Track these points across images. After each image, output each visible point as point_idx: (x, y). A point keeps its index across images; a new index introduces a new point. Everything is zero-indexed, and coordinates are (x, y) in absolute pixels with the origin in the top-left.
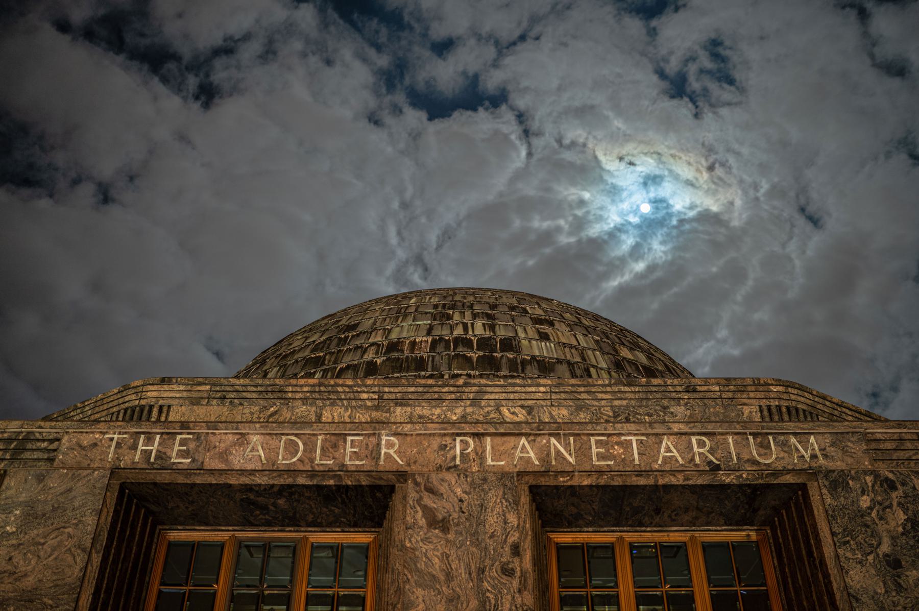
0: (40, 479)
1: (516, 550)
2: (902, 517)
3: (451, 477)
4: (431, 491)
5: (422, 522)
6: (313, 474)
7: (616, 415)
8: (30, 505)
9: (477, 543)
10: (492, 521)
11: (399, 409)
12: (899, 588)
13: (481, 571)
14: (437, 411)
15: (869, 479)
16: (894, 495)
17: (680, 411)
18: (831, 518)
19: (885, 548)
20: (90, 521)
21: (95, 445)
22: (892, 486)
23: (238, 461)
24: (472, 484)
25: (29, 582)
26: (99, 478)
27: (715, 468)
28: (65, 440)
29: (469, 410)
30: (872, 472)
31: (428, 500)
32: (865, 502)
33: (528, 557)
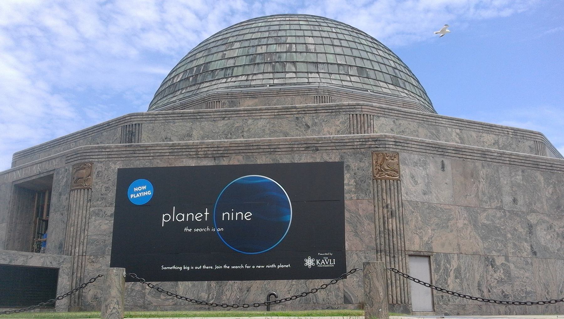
2: (65, 180)
17: (105, 134)
19: (60, 191)
30: (64, 167)
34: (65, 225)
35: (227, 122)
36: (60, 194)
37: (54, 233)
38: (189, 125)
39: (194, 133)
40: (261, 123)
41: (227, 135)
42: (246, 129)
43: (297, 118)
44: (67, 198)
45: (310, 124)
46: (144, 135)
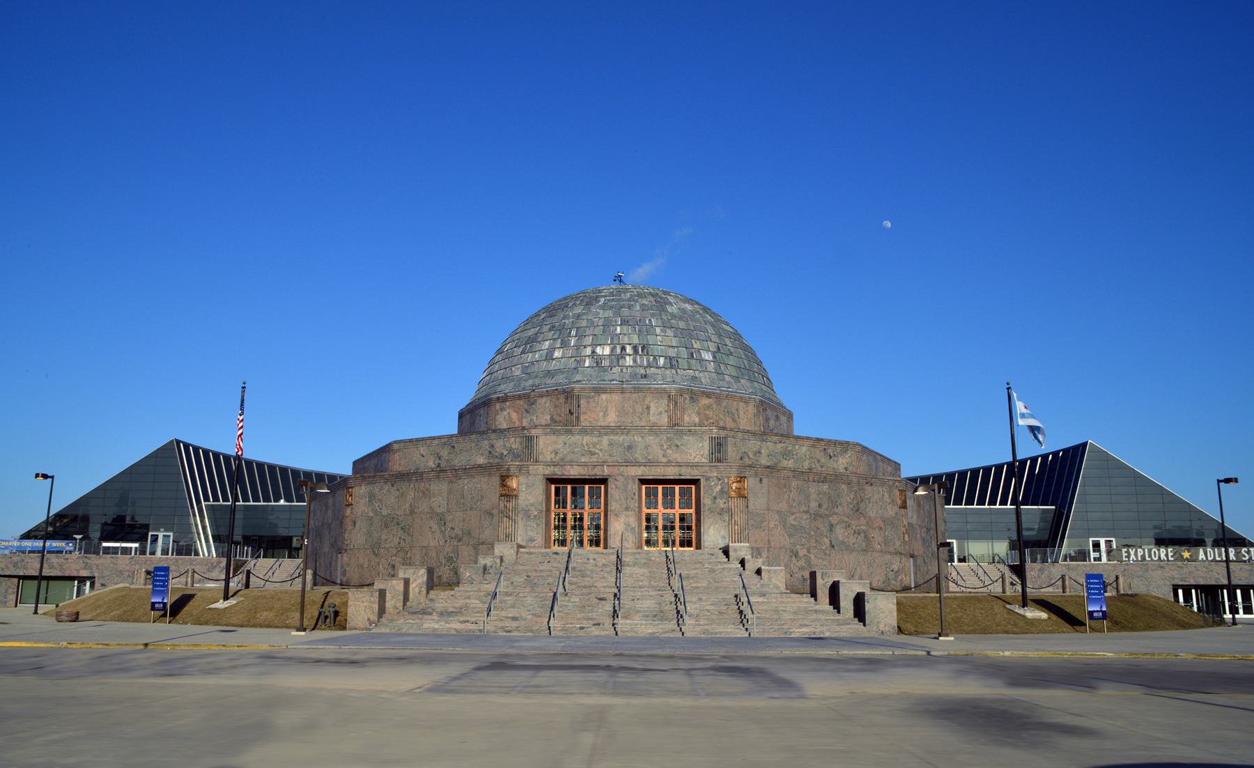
0: (527, 477)
1: (634, 494)
2: (720, 487)
3: (620, 477)
4: (616, 480)
5: (614, 487)
6: (590, 475)
7: (667, 439)
8: (526, 484)
9: (626, 492)
10: (630, 487)
11: (605, 437)
12: (715, 503)
13: (627, 498)
14: (616, 437)
15: (715, 478)
16: (720, 482)
18: (704, 487)
19: (714, 494)
20: (541, 487)
21: (538, 468)
22: (720, 480)
23: (572, 473)
24: (625, 479)
25: (531, 501)
26: (541, 477)
27: (680, 475)
28: (531, 467)
29: (626, 437)
30: (717, 477)
31: (616, 482)
32: (713, 484)
33: (637, 496)
34: (727, 524)
35: (783, 445)
36: (715, 498)
37: (712, 527)
38: (759, 443)
39: (763, 451)
40: (804, 449)
41: (783, 456)
42: (795, 453)
43: (825, 449)
44: (725, 503)
45: (831, 455)
46: (730, 449)
